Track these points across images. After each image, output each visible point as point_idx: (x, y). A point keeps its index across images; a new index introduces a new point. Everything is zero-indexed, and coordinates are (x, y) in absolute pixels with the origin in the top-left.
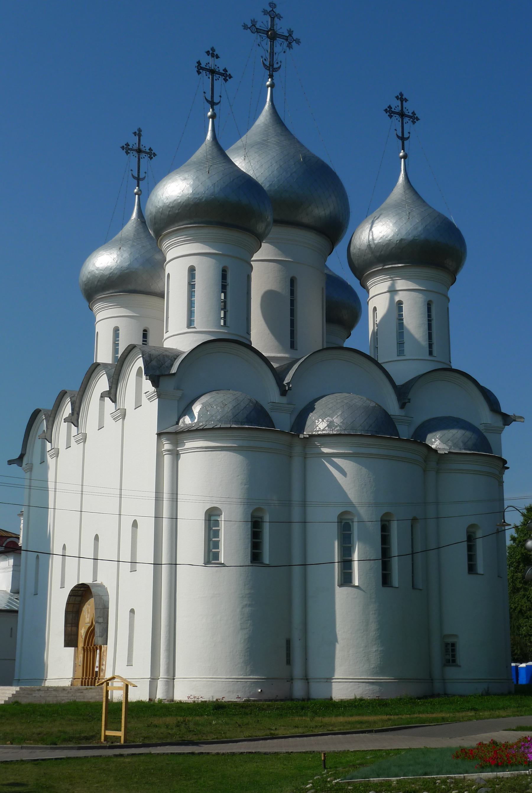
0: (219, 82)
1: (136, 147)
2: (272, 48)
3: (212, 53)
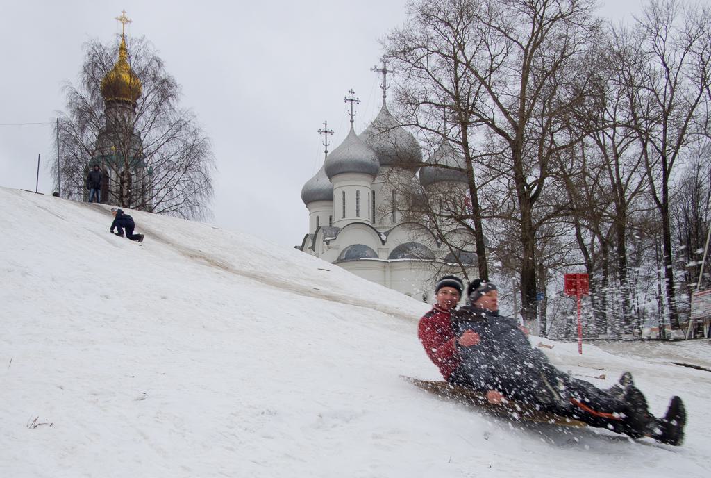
0: (355, 104)
1: (324, 130)
2: (385, 77)
3: (352, 92)
